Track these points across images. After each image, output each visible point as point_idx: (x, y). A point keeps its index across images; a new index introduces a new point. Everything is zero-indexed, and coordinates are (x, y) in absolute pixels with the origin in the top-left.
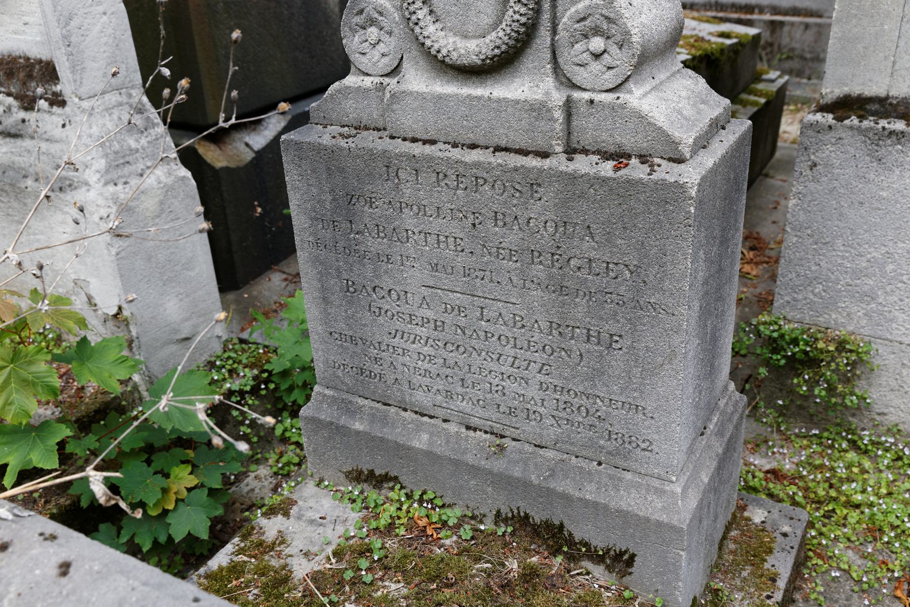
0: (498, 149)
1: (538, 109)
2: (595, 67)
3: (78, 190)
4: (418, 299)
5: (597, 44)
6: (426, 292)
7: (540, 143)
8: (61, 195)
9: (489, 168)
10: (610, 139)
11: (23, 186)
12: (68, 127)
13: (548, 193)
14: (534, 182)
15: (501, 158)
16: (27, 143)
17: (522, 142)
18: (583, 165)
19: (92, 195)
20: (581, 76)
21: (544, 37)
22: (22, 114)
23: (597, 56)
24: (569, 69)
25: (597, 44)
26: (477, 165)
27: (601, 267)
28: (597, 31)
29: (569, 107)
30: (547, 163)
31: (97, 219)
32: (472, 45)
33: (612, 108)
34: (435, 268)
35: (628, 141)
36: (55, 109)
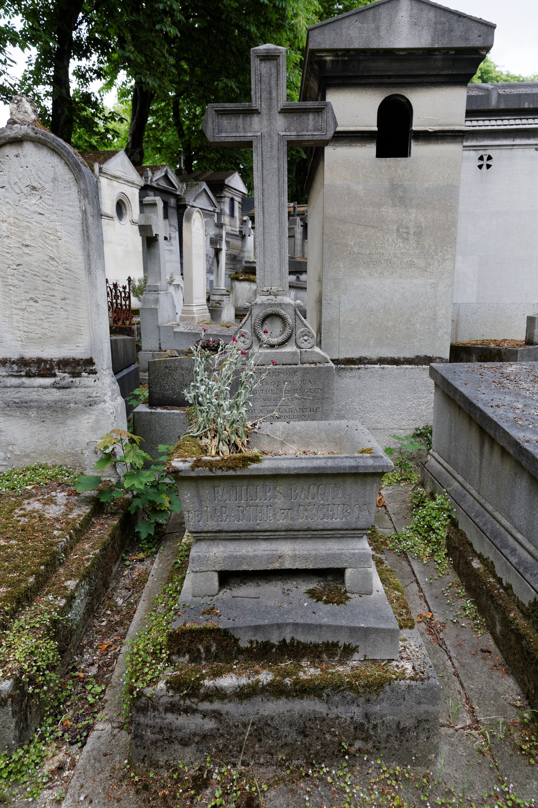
0: (283, 365)
1: (294, 353)
2: (306, 343)
3: (95, 407)
4: (259, 411)
5: (306, 338)
6: (261, 408)
7: (295, 362)
8: (91, 407)
9: (283, 369)
10: (310, 360)
11: (68, 407)
12: (97, 381)
13: (299, 374)
14: (295, 371)
15: (285, 367)
16: (73, 390)
17: (289, 362)
18: (306, 366)
19: (107, 405)
20: (302, 345)
21: (293, 337)
22: (71, 379)
23: (306, 341)
24: (299, 344)
25: (306, 338)
26: (279, 369)
27: (313, 390)
28: (306, 335)
29: (301, 352)
30: (298, 366)
31: (109, 413)
32: (276, 339)
33: (311, 352)
34: (265, 400)
35: (315, 360)
36: (91, 375)
